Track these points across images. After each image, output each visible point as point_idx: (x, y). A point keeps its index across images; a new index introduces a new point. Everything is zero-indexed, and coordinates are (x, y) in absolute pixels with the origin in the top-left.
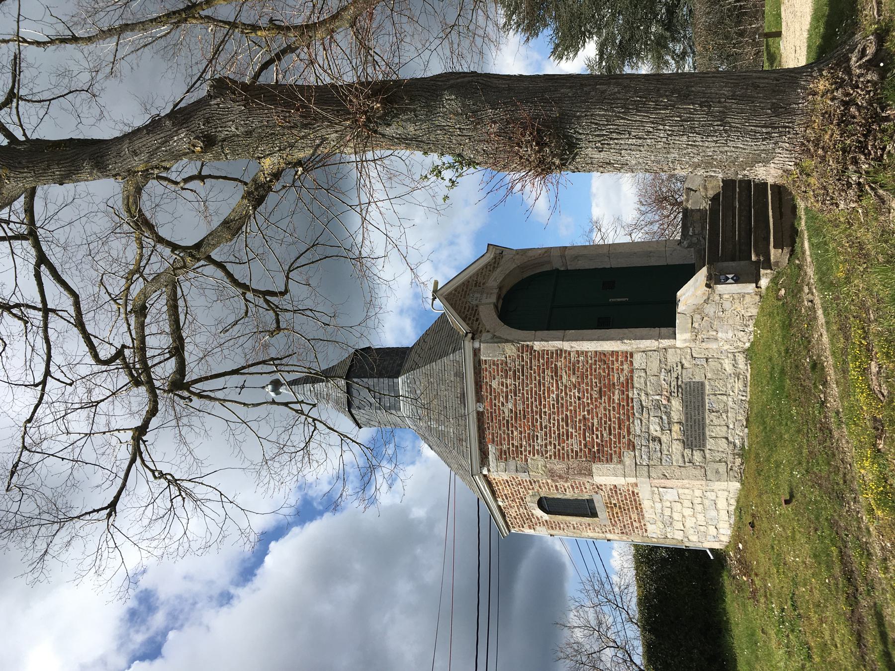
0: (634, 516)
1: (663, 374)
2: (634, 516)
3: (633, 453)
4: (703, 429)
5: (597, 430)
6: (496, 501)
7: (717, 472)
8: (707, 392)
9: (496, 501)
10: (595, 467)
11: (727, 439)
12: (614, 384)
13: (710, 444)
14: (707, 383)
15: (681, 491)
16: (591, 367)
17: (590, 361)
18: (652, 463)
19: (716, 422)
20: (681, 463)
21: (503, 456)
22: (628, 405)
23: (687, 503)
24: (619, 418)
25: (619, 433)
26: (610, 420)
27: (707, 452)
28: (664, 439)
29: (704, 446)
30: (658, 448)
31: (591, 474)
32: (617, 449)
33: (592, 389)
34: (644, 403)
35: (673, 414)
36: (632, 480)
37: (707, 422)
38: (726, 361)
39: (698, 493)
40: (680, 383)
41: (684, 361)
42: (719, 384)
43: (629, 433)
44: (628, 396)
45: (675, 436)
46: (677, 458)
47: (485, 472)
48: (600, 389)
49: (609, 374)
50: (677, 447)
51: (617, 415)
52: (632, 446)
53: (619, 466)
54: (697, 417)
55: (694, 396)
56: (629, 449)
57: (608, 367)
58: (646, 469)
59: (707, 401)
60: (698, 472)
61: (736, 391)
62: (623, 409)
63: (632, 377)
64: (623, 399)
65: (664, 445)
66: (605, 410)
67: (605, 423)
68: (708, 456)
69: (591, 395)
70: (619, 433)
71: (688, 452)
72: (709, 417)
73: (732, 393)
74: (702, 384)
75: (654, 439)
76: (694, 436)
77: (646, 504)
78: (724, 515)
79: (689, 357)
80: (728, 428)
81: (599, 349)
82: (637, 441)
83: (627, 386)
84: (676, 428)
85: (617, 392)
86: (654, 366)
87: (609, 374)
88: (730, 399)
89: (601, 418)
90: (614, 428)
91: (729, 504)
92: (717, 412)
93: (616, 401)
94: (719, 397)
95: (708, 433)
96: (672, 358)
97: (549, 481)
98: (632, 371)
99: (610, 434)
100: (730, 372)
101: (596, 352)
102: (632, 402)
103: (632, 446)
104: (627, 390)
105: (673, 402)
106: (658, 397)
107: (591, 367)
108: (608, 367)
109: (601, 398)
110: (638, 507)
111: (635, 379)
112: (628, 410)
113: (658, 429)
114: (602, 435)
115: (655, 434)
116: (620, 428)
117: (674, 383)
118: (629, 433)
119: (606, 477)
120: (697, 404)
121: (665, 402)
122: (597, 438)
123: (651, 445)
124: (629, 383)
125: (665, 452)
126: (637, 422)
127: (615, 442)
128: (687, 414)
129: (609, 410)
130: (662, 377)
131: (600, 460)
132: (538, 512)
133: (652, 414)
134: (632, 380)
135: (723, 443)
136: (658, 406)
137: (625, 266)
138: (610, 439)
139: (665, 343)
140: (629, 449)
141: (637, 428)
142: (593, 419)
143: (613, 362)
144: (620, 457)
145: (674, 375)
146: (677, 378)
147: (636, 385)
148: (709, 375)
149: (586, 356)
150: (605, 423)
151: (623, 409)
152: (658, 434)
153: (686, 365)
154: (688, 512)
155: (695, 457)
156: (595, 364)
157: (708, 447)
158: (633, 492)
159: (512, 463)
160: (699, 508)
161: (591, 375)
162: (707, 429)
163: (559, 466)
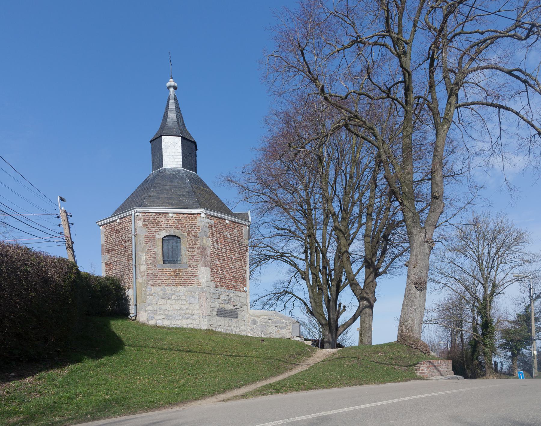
0: (169, 282)
2: (169, 282)
6: (173, 213)
7: (210, 320)
9: (173, 213)
10: (208, 269)
13: (219, 319)
20: (213, 306)
21: (210, 226)
28: (220, 301)
31: (206, 266)
39: (196, 312)
42: (237, 324)
43: (221, 286)
47: (203, 215)
50: (217, 306)
53: (210, 280)
71: (216, 309)
75: (219, 296)
76: (222, 313)
78: (180, 322)
80: (224, 326)
82: (218, 289)
84: (223, 306)
86: (242, 300)
91: (187, 325)
96: (245, 307)
97: (198, 246)
110: (177, 284)
115: (221, 296)
118: (221, 286)
119: (204, 274)
121: (231, 303)
125: (215, 300)
126: (225, 290)
132: (164, 233)
136: (230, 299)
141: (223, 289)
147: (237, 292)
159: (207, 230)
163: (208, 252)
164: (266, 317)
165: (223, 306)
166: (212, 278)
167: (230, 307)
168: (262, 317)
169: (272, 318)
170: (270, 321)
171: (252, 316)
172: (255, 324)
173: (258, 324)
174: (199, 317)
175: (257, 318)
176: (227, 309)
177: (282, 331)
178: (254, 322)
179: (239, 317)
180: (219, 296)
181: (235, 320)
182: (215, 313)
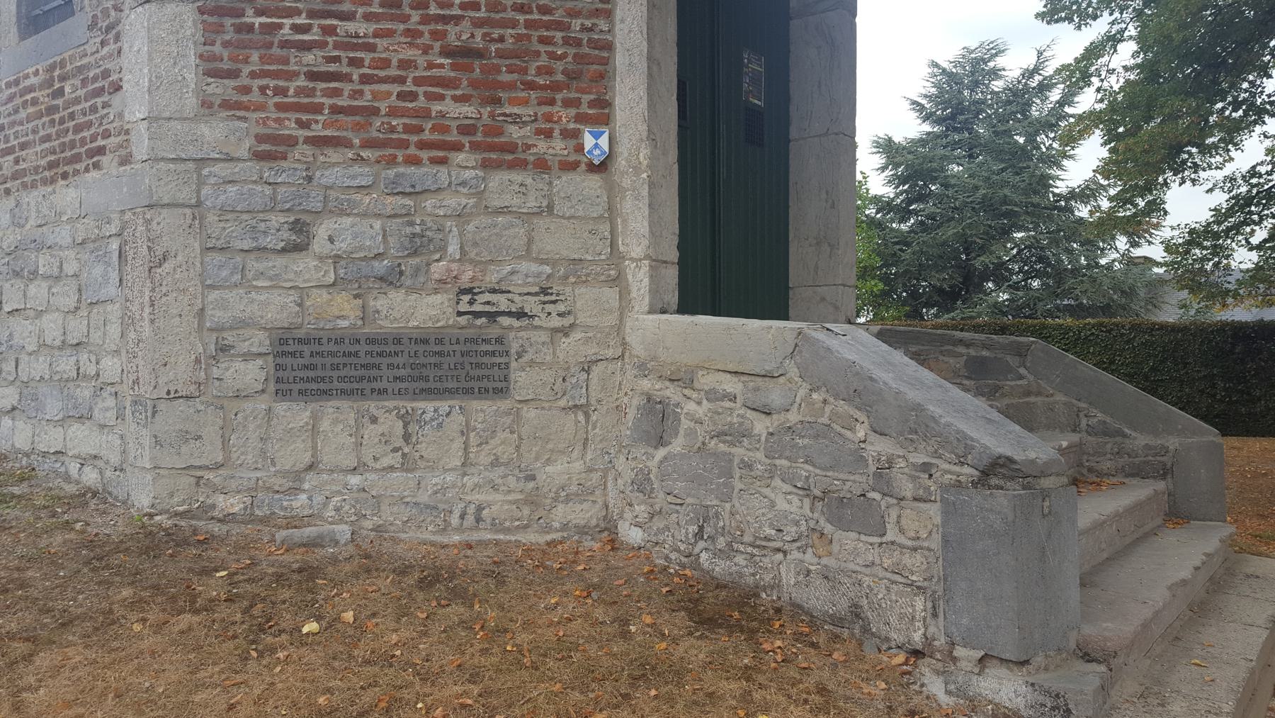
1: (534, 268)
3: (243, 152)
4: (345, 393)
5: (329, 31)
8: (475, 405)
11: (311, 467)
12: (497, 101)
13: (295, 414)
14: (504, 405)
15: (114, 310)
16: (559, 26)
17: (576, 24)
18: (211, 218)
19: (370, 432)
20: (216, 316)
22: (422, 145)
23: (77, 328)
24: (375, 112)
25: (317, 109)
26: (365, 79)
27: (261, 404)
28: (305, 268)
29: (282, 394)
30: (269, 241)
32: (255, 96)
33: (478, 24)
34: (429, 203)
35: (396, 296)
36: (141, 147)
37: (372, 406)
38: (578, 466)
39: (111, 367)
40: (505, 321)
41: (577, 335)
42: (502, 445)
44: (457, 147)
45: (319, 298)
46: (235, 304)
48: (479, 54)
49: (531, 86)
51: (383, 106)
52: (271, 150)
53: (191, 103)
54: (385, 372)
55: (463, 364)
56: (260, 139)
57: (556, 87)
58: (186, 195)
59: (444, 406)
60: (181, 373)
61: (478, 497)
62: (408, 129)
63: (520, 165)
64: (445, 129)
65: (280, 261)
66: (405, 64)
67: (354, 62)
68: (248, 406)
69: (457, 19)
70: (317, 109)
71: (258, 341)
72: (386, 417)
73: (469, 481)
74: (501, 392)
75: (299, 227)
76: (314, 366)
77: (67, 196)
78: (52, 439)
79: (591, 350)
81: (620, 59)
82: (288, 173)
83: (492, 148)
85: (468, 110)
87: (531, 86)
88: (450, 478)
89: (371, 48)
90: (336, 93)
92: (407, 437)
93: (436, 107)
94: (458, 444)
95: (330, 406)
96: (589, 302)
98: (542, 165)
99: (313, 76)
100: (541, 477)
101: (609, 47)
102: (434, 161)
103: (271, 150)
104: (475, 147)
105: (438, 298)
106: (453, 248)
107: (559, 26)
108: (556, 87)
109: (446, 52)
110: (60, 168)
111: (517, 177)
112: (404, 144)
113: (342, 246)
114: (306, 47)
115: (322, 231)
116: (335, 110)
117: (502, 302)
120: (431, 373)
121: (438, 269)
122: (297, 29)
123: (276, 220)
124: (499, 153)
125: (254, 265)
126: (363, 175)
127: (282, 92)
128: (398, 341)
129: (402, 80)
130: (525, 266)
131: (211, 32)
133: (394, 224)
134: (512, 166)
135: (294, 454)
136: (419, 245)
137: (792, 178)
138: (292, 76)
139: (639, 280)
140: (260, 139)
141: (337, 171)
142: (368, 17)
143: (575, 103)
144: (226, 105)
145: (531, 305)
146: (520, 315)
147: (498, 179)
148: (530, 413)
149: (597, 13)
150: (354, 62)
151: (408, 129)
152: (319, 244)
153: (565, 343)
154: (51, 327)
155: (239, 365)
156: (567, 41)
157: (281, 407)
158: (101, 151)
160: (66, 365)
161: (529, 25)
162: (344, 404)
164: (731, 385)
165: (341, 311)
166: (217, 88)
167: (422, 309)
168: (706, 381)
169: (775, 395)
170: (761, 426)
171: (643, 369)
172: (661, 442)
173: (677, 445)
174: (120, 416)
175: (672, 393)
176: (387, 325)
177: (851, 546)
178: (658, 422)
179: (523, 380)
180: (299, 227)
181: (483, 410)
182: (251, 374)
